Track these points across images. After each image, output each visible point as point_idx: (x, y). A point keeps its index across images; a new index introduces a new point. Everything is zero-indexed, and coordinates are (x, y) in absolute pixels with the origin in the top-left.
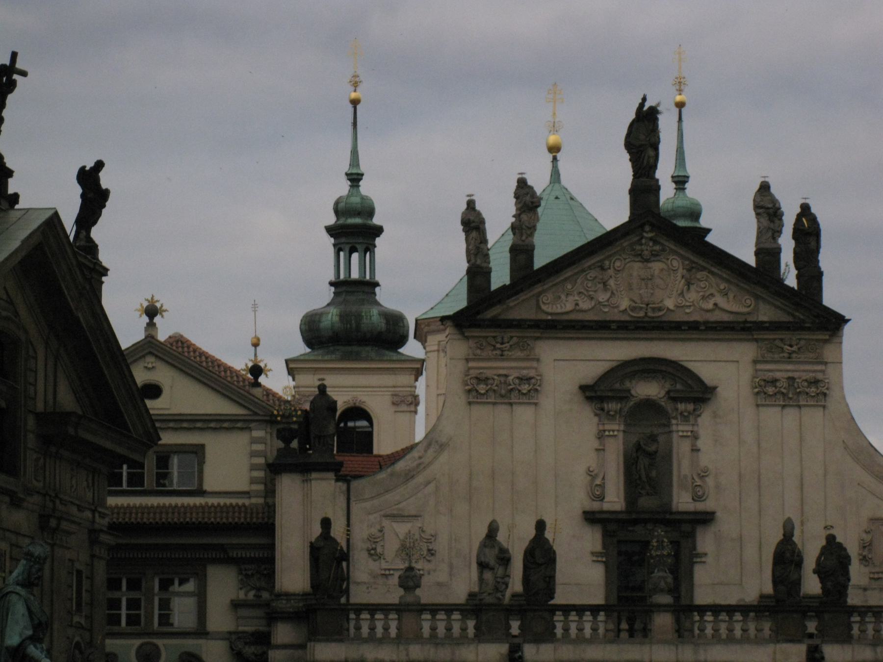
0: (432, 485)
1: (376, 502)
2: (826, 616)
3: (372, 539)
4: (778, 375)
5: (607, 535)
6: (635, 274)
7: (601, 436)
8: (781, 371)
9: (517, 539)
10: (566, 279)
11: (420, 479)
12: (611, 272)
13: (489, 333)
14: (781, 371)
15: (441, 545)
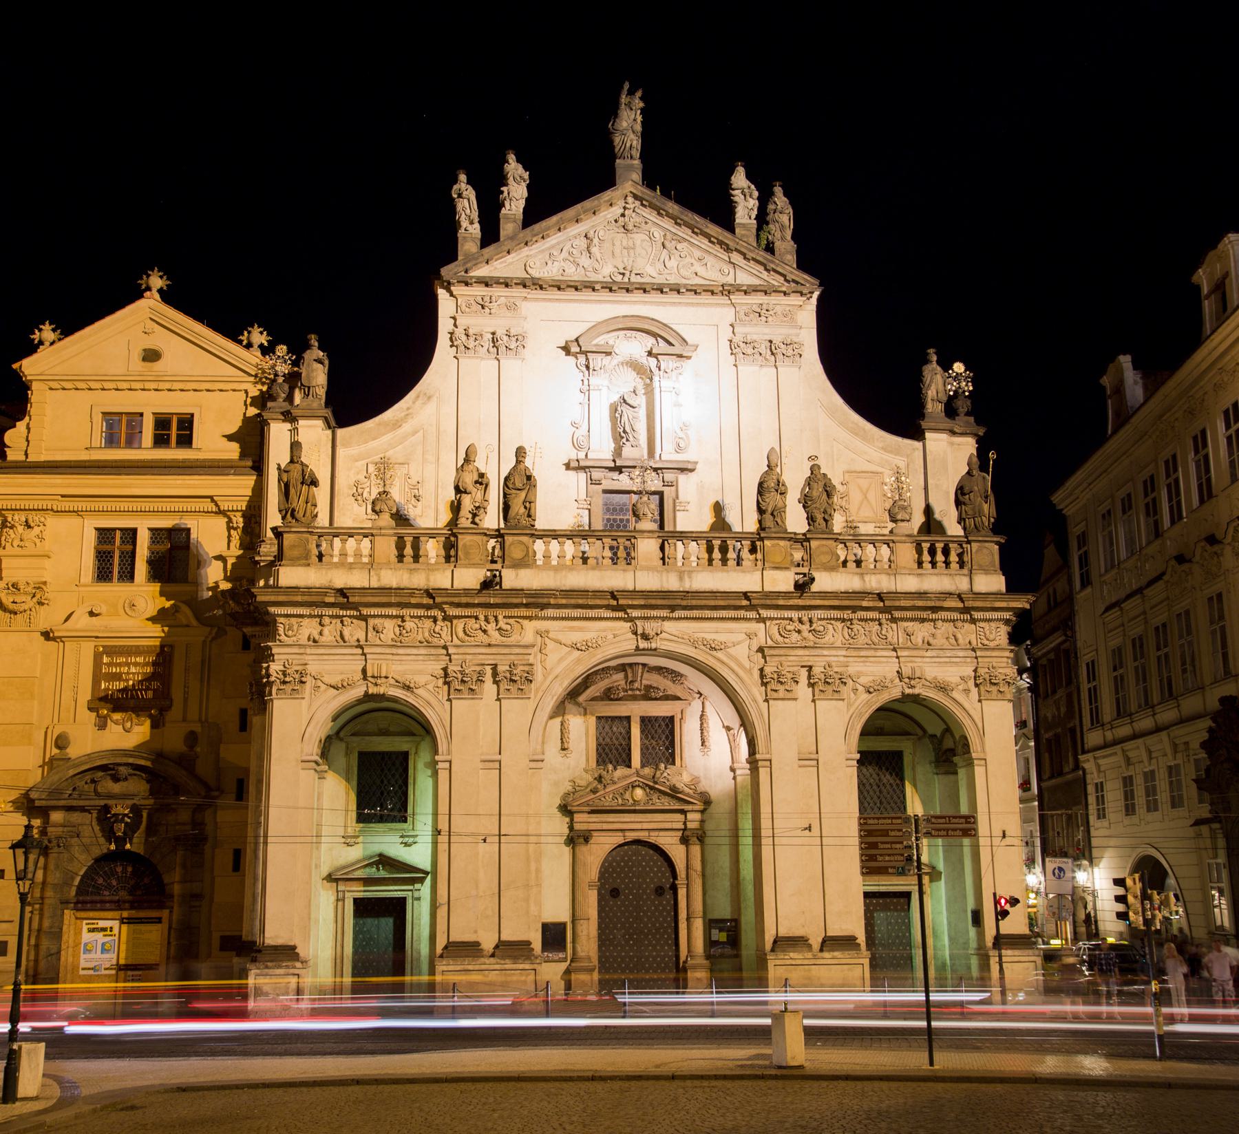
0: (420, 434)
1: (363, 448)
2: (814, 544)
3: (357, 485)
4: (755, 337)
5: (594, 482)
6: (618, 243)
7: (587, 391)
8: (759, 332)
9: (495, 468)
10: (553, 247)
11: (407, 427)
12: (596, 241)
13: (479, 291)
14: (759, 332)
15: (427, 491)
